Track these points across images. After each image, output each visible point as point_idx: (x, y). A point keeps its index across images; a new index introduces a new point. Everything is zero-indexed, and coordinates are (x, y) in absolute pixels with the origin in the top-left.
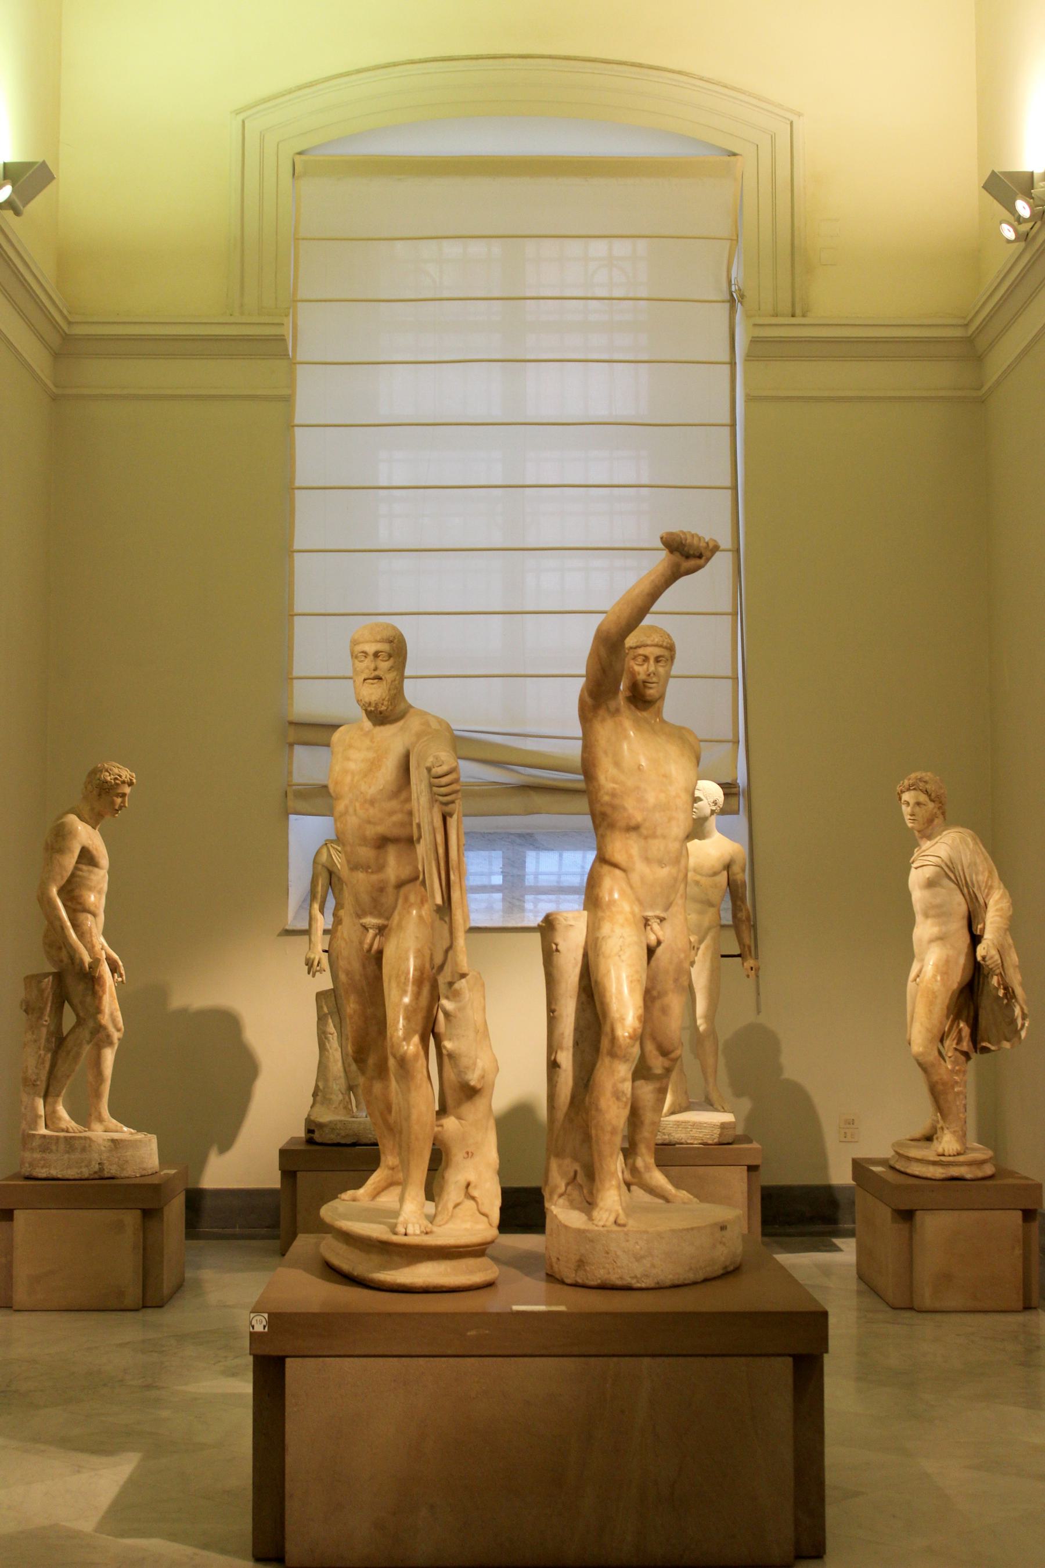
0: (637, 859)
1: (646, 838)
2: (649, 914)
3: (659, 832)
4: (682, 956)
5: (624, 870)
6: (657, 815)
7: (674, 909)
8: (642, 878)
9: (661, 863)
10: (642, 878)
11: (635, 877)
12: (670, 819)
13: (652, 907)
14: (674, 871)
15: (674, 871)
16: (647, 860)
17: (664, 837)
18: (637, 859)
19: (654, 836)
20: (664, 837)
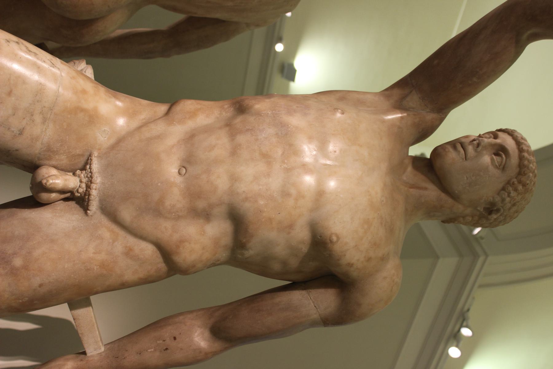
0: (190, 125)
1: (228, 124)
2: (96, 166)
3: (241, 139)
4: (18, 262)
5: (167, 113)
6: (271, 131)
7: (107, 230)
8: (159, 137)
9: (187, 163)
10: (159, 137)
11: (160, 127)
12: (266, 157)
13: (107, 168)
14: (176, 198)
15: (176, 198)
16: (190, 138)
17: (234, 152)
18: (190, 125)
19: (232, 135)
20: (234, 152)
